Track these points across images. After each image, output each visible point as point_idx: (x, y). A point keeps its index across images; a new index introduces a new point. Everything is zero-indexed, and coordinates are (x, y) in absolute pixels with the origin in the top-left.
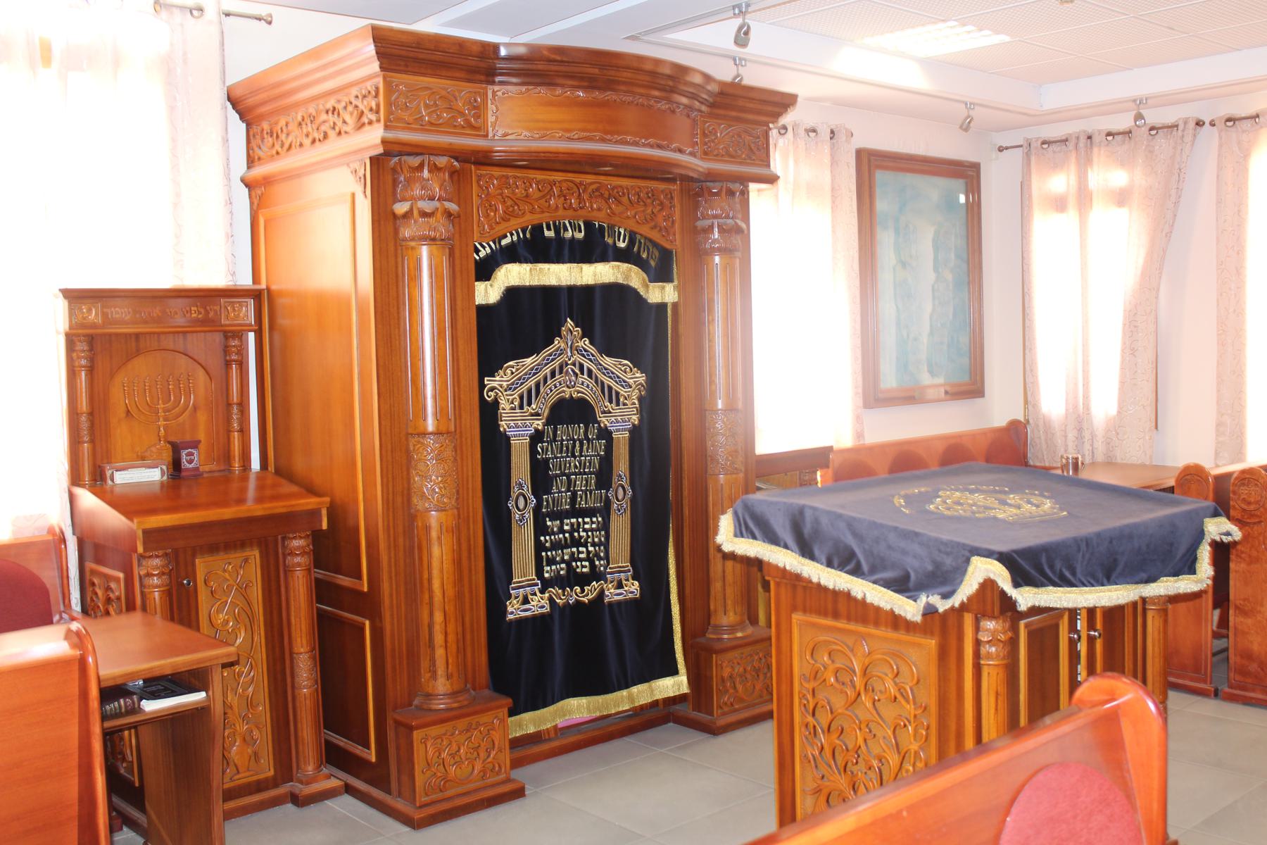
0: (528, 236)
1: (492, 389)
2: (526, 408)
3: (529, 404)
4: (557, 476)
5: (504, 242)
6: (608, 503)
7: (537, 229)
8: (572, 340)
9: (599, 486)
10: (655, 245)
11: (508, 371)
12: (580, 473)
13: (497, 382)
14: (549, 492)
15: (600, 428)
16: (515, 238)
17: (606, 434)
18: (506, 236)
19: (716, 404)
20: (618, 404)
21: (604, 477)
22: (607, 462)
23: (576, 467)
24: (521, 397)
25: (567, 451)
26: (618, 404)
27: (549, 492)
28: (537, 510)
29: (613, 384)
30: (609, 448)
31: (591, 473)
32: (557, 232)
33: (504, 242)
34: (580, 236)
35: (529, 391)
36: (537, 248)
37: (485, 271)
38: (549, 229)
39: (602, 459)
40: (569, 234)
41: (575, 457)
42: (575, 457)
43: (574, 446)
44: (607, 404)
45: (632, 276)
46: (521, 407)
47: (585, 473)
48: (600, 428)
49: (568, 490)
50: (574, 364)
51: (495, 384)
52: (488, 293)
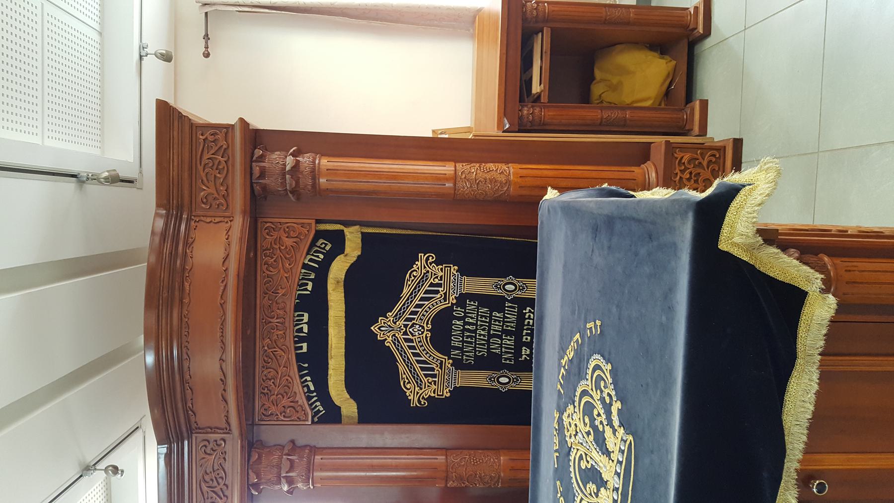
0: (306, 365)
1: (419, 402)
2: (436, 372)
3: (433, 369)
4: (489, 349)
5: (312, 388)
6: (515, 300)
7: (300, 358)
8: (386, 329)
9: (502, 310)
10: (313, 244)
11: (408, 386)
12: (489, 327)
13: (416, 393)
14: (500, 356)
15: (457, 305)
16: (309, 378)
17: (462, 299)
18: (308, 386)
19: (449, 188)
20: (440, 285)
21: (494, 303)
22: (483, 300)
23: (483, 330)
24: (426, 376)
25: (471, 337)
26: (440, 285)
27: (500, 356)
28: (511, 368)
29: (423, 290)
30: (473, 297)
31: (491, 316)
32: (302, 340)
33: (312, 388)
34: (306, 316)
35: (422, 369)
36: (315, 362)
37: (332, 415)
38: (301, 348)
39: (481, 305)
40: (306, 329)
41: (475, 331)
42: (477, 329)
43: (468, 330)
44: (439, 296)
45: (339, 269)
46: (434, 376)
47: (490, 323)
48: (457, 305)
49: (500, 337)
50: (406, 326)
51: (416, 399)
52: (349, 407)
